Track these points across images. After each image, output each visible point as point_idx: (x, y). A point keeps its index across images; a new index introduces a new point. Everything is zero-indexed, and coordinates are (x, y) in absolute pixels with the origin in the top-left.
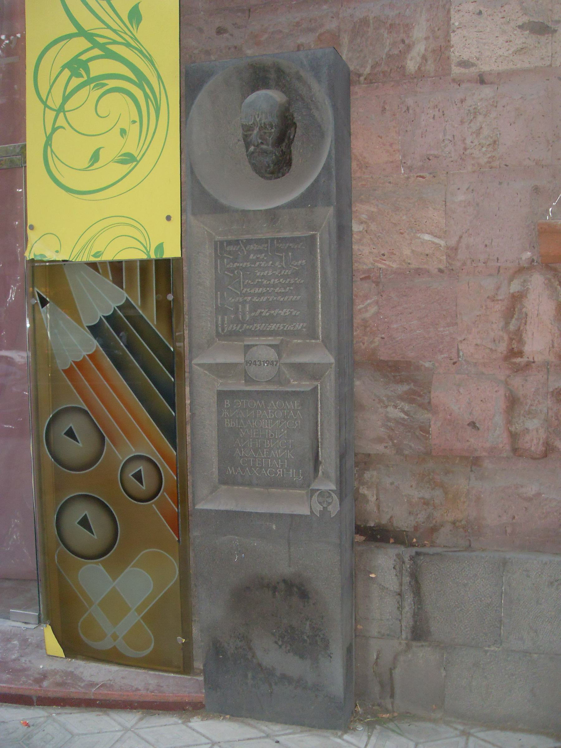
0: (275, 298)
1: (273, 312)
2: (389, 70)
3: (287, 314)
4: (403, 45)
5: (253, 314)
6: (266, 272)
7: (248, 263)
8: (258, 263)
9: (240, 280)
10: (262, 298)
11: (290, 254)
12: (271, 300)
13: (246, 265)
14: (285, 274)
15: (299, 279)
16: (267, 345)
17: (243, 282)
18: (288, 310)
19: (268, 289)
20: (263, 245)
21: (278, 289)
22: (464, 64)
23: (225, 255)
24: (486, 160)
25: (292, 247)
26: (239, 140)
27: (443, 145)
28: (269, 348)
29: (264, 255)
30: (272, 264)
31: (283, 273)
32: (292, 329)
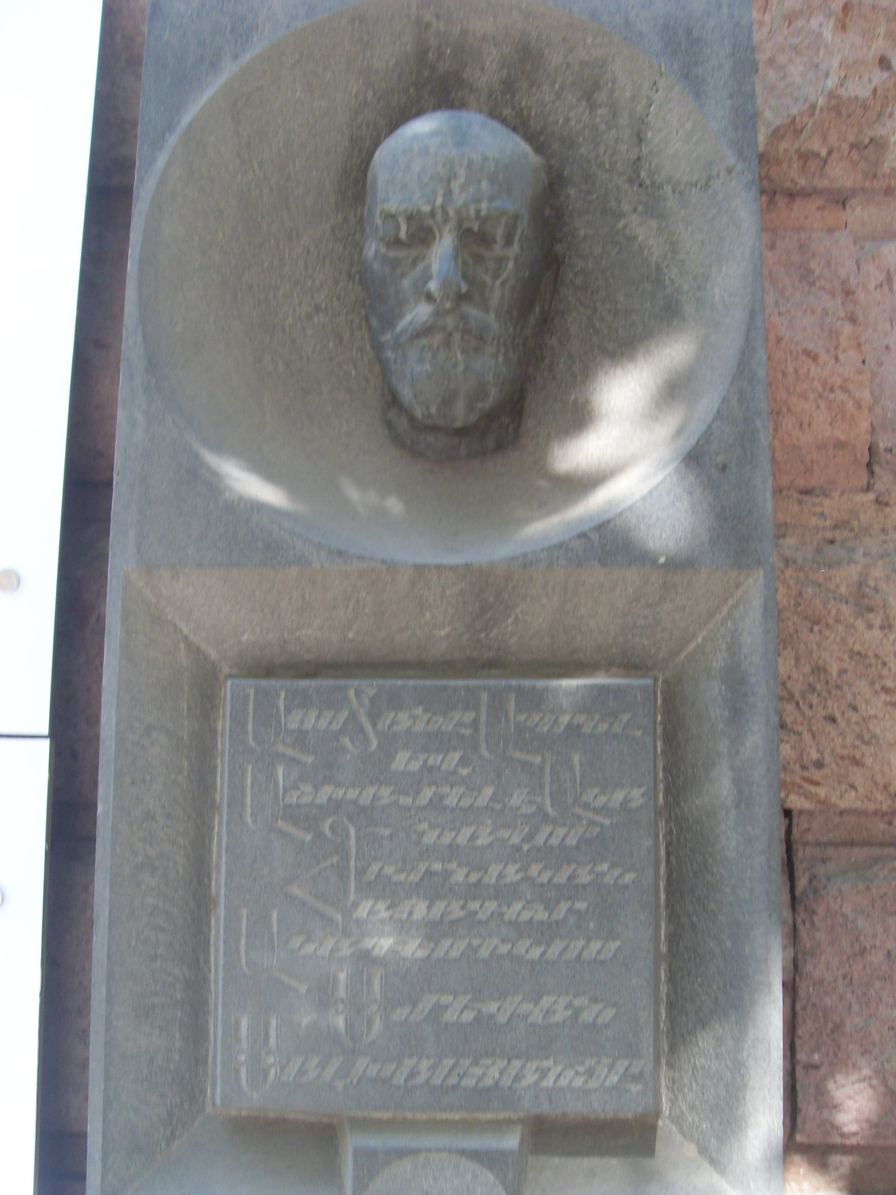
0: (504, 949)
1: (493, 1007)
2: (824, 153)
3: (559, 1017)
4: (886, 75)
5: (400, 1014)
6: (467, 832)
7: (385, 792)
8: (428, 793)
9: (346, 858)
10: (446, 943)
11: (576, 759)
12: (484, 953)
13: (375, 798)
14: (554, 841)
15: (613, 866)
16: (463, 1153)
17: (361, 873)
18: (562, 1002)
19: (474, 905)
20: (457, 716)
21: (518, 906)
23: (281, 748)
25: (587, 729)
26: (317, 308)
28: (470, 1165)
29: (456, 756)
30: (493, 799)
31: (540, 840)
32: (578, 1082)
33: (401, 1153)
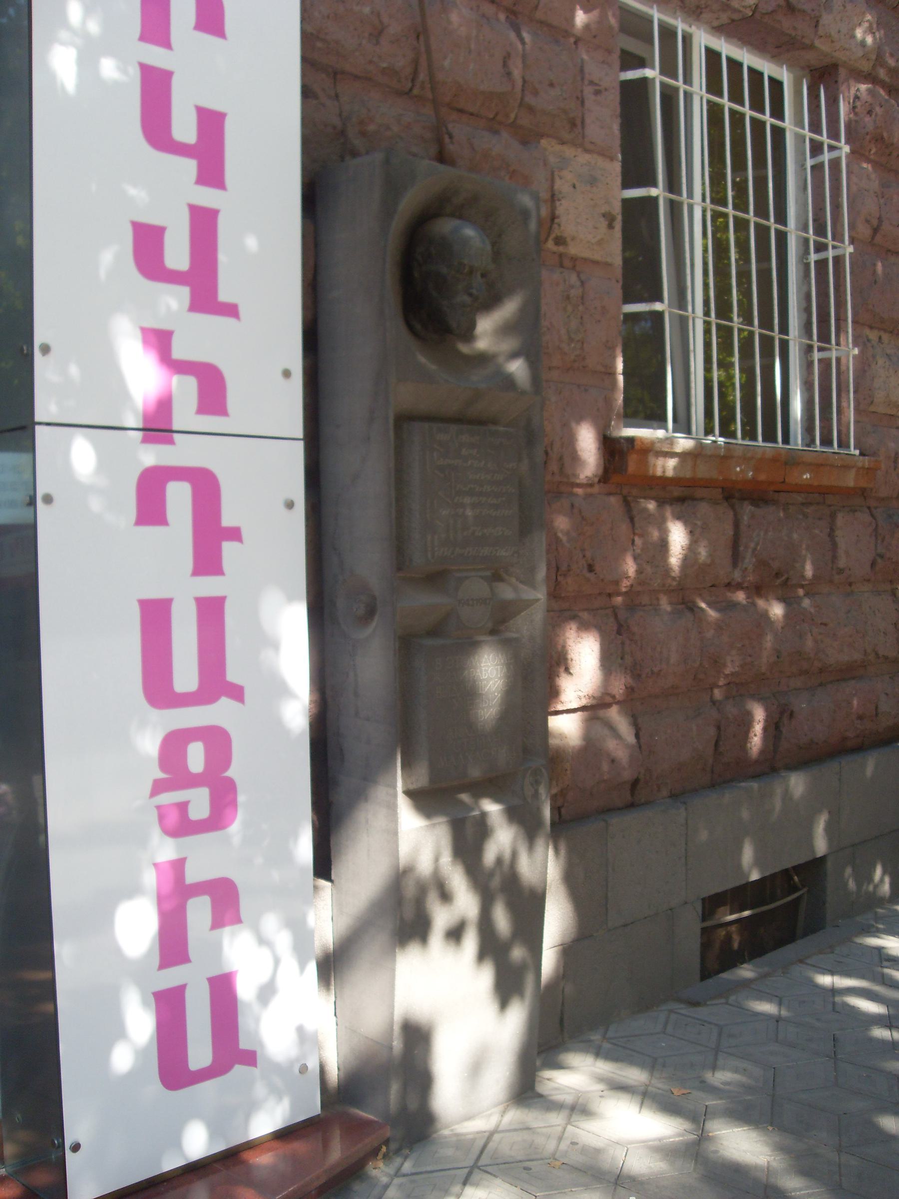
22: (560, 241)
33: (467, 578)
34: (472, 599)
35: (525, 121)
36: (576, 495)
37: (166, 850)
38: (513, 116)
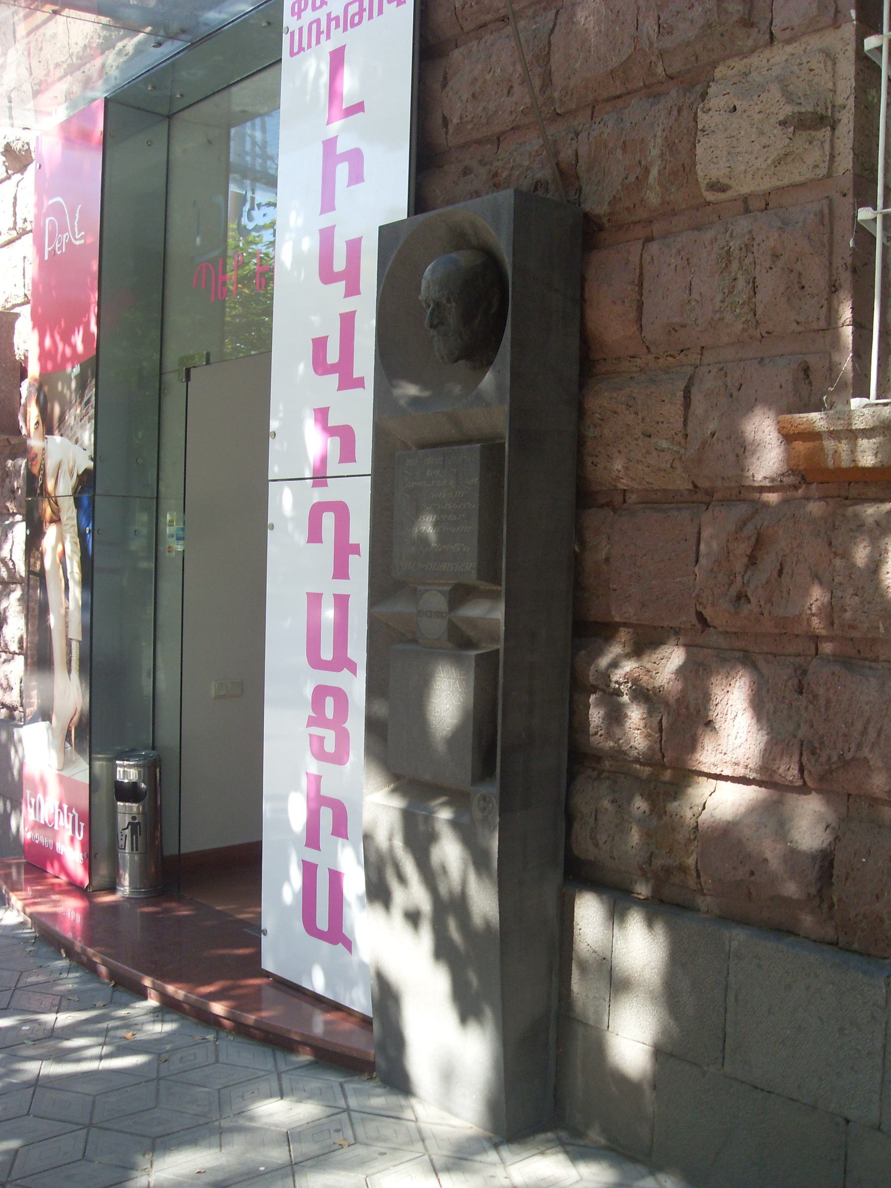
22: (717, 187)
24: (741, 327)
27: (688, 308)
33: (426, 591)
34: (431, 611)
35: (677, 65)
36: (766, 505)
37: (313, 766)
38: (660, 70)
